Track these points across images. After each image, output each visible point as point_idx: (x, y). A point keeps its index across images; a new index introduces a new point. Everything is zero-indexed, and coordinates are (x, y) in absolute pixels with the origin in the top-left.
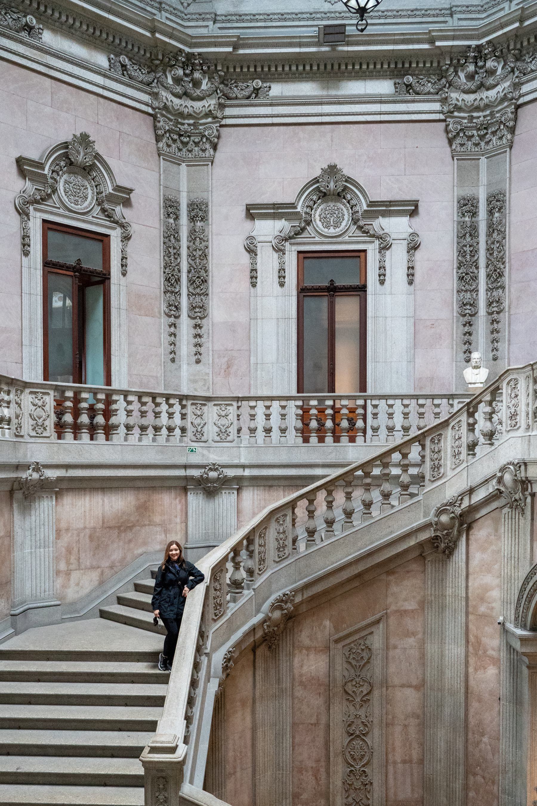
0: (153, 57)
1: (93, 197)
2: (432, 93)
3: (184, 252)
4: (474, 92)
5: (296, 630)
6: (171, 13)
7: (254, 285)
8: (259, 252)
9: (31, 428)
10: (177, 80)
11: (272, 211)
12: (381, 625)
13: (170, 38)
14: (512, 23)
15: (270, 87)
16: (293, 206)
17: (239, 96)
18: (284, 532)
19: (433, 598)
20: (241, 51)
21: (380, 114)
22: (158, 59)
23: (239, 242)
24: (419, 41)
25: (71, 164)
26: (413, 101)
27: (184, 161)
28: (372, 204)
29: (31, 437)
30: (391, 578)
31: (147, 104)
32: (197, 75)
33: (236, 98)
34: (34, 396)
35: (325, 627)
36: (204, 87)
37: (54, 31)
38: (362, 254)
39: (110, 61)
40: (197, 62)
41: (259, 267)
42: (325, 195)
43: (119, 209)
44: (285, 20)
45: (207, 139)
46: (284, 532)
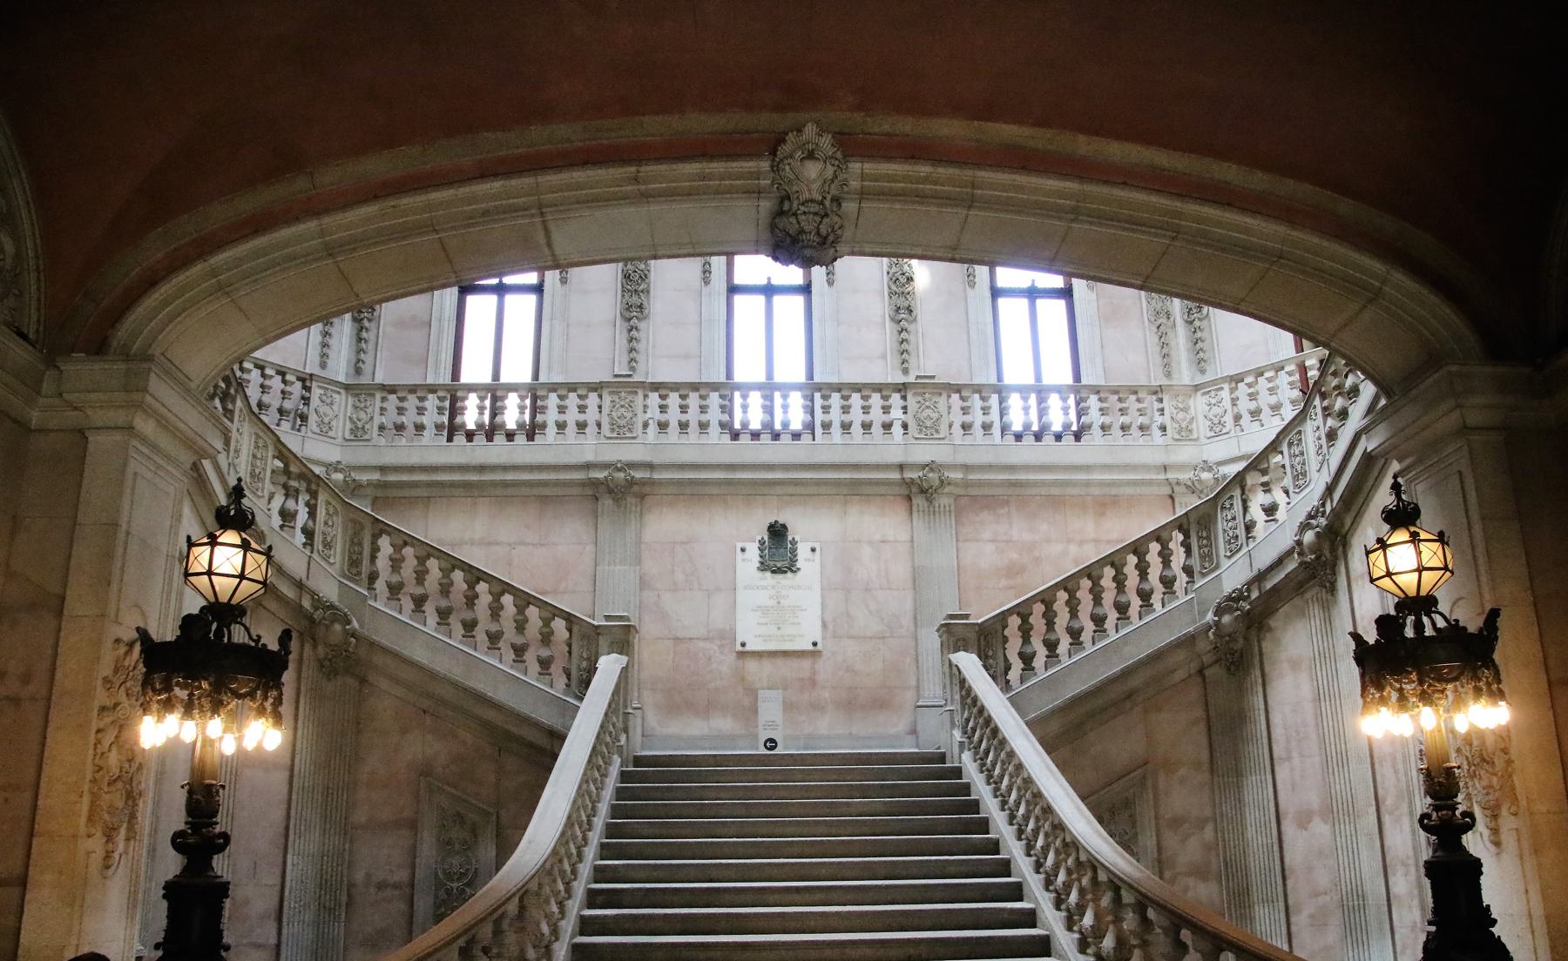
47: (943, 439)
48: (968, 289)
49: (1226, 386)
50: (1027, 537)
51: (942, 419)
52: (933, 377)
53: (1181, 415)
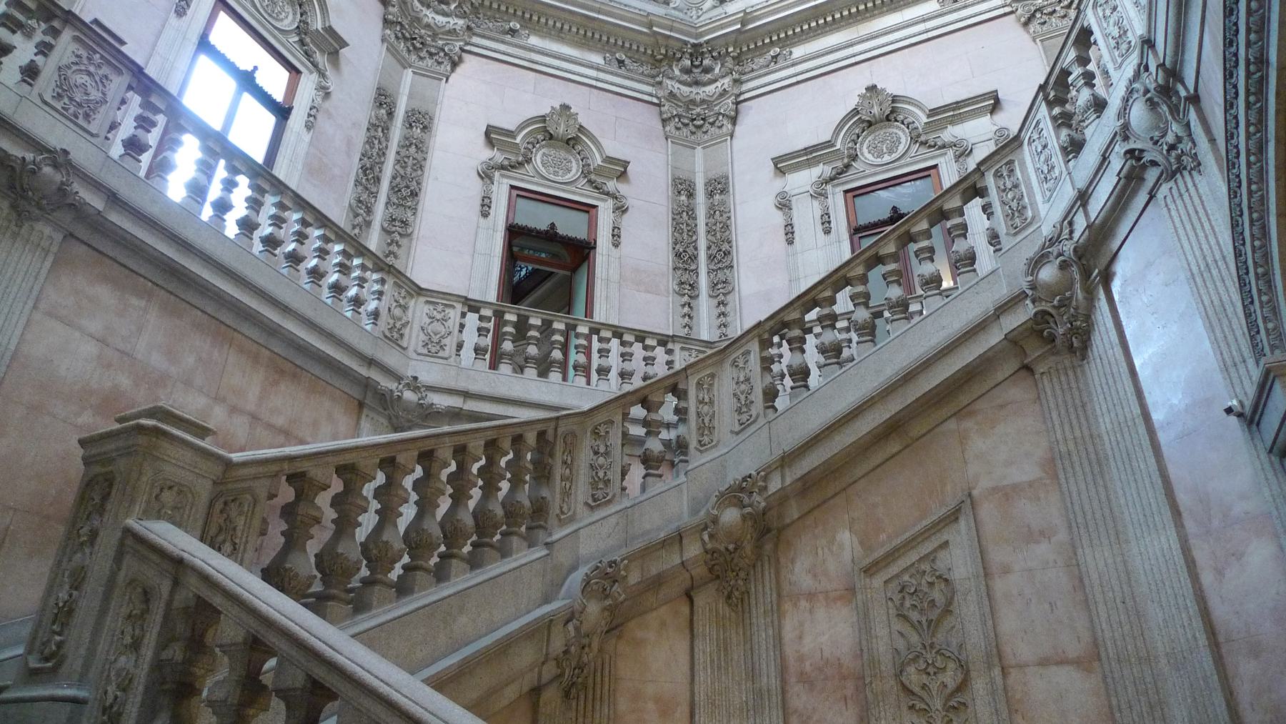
1: (578, 171)
3: (702, 229)
5: (782, 560)
7: (790, 242)
8: (794, 207)
9: (421, 344)
11: (805, 158)
12: (962, 523)
15: (791, 53)
16: (829, 144)
18: (747, 380)
19: (1072, 446)
21: (927, 31)
22: (661, 54)
23: (769, 201)
25: (551, 137)
27: (699, 145)
28: (933, 112)
29: (419, 354)
30: (969, 424)
31: (651, 95)
32: (706, 62)
33: (753, 70)
34: (432, 308)
35: (841, 547)
37: (541, 37)
38: (932, 171)
39: (605, 58)
40: (705, 50)
41: (795, 221)
42: (870, 124)
43: (611, 185)
45: (723, 115)
46: (747, 380)
47: (92, 135)
48: (173, 15)
49: (459, 307)
50: (157, 361)
51: (103, 109)
52: (122, 43)
53: (397, 312)
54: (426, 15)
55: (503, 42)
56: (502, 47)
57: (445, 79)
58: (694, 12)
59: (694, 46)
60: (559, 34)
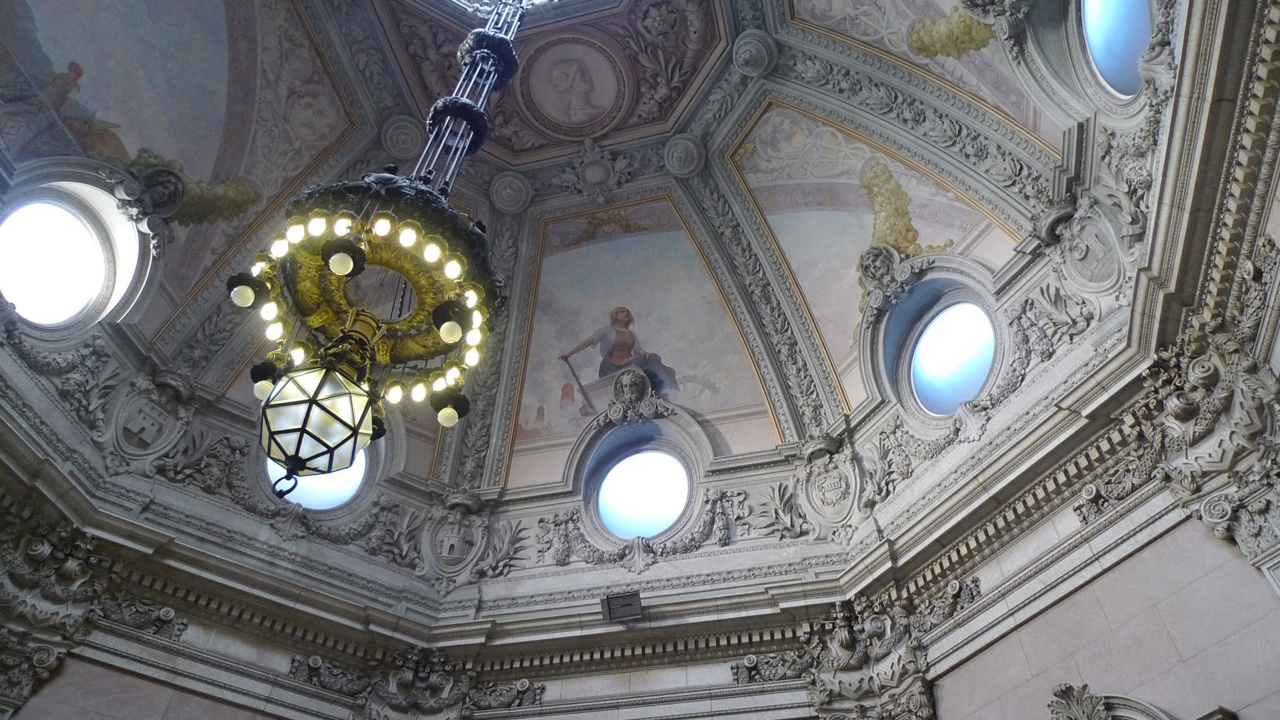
0: (368, 657)
2: (790, 678)
4: (858, 668)
6: (417, 603)
10: (404, 686)
13: (395, 629)
14: (882, 563)
15: (543, 689)
17: (493, 704)
20: (498, 642)
24: (754, 605)
26: (763, 692)
36: (445, 695)
37: (207, 627)
40: (435, 660)
44: (574, 598)
54: (24, 602)
55: (139, 640)
56: (134, 649)
57: (11, 711)
58: (444, 584)
59: (423, 650)
60: (234, 627)
